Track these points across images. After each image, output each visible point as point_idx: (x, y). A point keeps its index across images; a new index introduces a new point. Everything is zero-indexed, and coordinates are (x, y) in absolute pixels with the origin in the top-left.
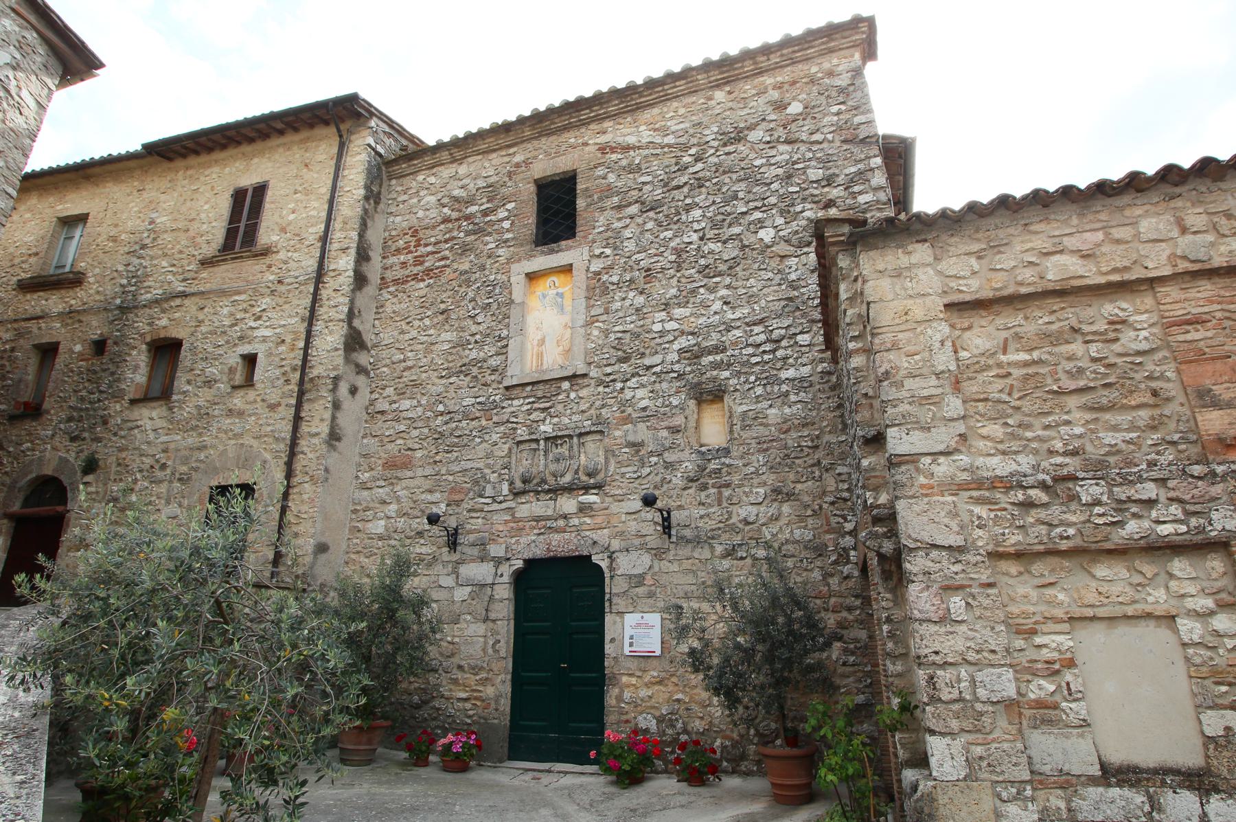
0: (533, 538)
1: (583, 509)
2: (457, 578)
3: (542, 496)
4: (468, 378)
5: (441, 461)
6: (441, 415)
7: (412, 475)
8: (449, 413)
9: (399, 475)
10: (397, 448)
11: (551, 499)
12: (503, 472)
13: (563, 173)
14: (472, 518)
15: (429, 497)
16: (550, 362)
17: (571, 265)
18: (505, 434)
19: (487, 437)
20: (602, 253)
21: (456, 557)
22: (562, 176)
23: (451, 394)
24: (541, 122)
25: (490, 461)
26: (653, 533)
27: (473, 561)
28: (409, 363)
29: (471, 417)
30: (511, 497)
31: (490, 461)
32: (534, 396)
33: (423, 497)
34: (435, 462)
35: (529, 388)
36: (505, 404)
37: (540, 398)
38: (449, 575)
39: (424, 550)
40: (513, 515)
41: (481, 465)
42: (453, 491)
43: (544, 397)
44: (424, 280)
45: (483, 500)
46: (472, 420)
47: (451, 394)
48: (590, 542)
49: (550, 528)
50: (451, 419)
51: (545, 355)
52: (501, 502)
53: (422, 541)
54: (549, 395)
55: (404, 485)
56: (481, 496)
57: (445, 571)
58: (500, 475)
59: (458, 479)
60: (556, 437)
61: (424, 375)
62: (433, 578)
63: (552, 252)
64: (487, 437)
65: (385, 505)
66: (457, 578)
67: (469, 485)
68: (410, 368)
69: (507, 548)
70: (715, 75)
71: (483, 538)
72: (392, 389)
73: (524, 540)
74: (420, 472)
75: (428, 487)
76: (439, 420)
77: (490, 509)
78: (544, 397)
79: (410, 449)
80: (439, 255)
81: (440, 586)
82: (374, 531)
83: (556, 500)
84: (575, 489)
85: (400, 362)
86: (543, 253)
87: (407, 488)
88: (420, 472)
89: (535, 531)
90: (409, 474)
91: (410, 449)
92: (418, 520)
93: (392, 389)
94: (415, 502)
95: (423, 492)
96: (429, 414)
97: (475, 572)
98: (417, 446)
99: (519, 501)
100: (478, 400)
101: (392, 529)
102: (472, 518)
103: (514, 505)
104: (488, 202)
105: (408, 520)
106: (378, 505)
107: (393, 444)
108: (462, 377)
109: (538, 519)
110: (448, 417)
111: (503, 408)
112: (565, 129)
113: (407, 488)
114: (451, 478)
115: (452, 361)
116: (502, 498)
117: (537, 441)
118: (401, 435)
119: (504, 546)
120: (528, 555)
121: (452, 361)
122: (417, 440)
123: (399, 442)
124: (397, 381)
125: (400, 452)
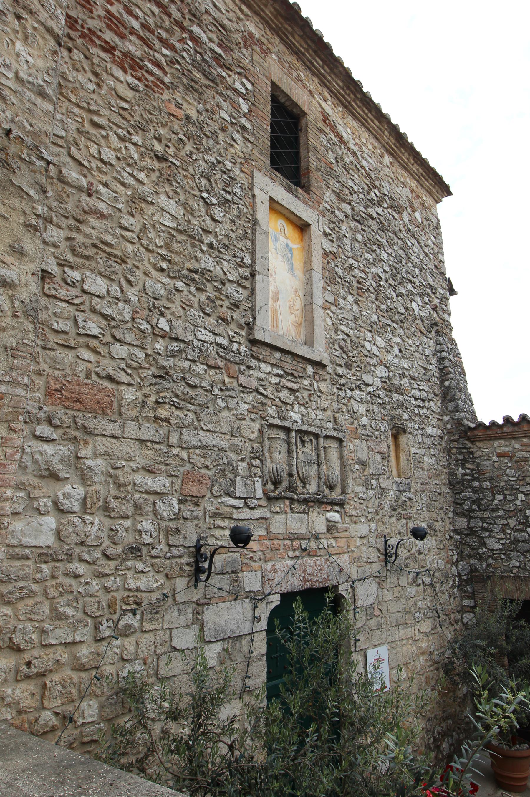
0: (290, 563)
1: (331, 527)
2: (202, 630)
3: (296, 505)
4: (202, 297)
5: (167, 421)
6: (163, 337)
7: (118, 432)
8: (177, 339)
9: (91, 424)
10: (83, 366)
11: (304, 512)
12: (254, 462)
13: (296, 105)
14: (217, 527)
15: (150, 483)
16: (285, 329)
17: (308, 225)
18: (254, 407)
19: (232, 404)
20: (330, 234)
21: (197, 595)
22: (287, 103)
23: (176, 307)
24: (286, 19)
25: (238, 442)
26: (377, 560)
27: (222, 599)
28: (102, 206)
29: (211, 362)
30: (264, 502)
31: (238, 442)
32: (283, 368)
33: (138, 478)
34: (157, 419)
35: (278, 355)
36: (253, 363)
37: (287, 374)
38: (187, 627)
39: (143, 583)
40: (268, 529)
41: (225, 444)
42: (187, 477)
43: (292, 375)
44: (125, 72)
45: (232, 502)
46: (210, 367)
47: (176, 307)
48: (337, 569)
49: (305, 550)
50: (180, 351)
51: (279, 312)
52: (253, 508)
53: (140, 566)
54: (296, 374)
55: (101, 448)
56: (229, 494)
57: (182, 621)
58: (250, 465)
59: (197, 460)
60: (306, 433)
61: (130, 248)
62: (162, 636)
63: (290, 191)
64: (232, 404)
65: (52, 483)
66: (202, 630)
67: (210, 473)
68: (101, 216)
69: (263, 577)
70: (392, 141)
71: (234, 561)
72: (62, 234)
73: (279, 565)
74: (131, 430)
75: (144, 462)
76: (160, 345)
77: (241, 516)
78: (292, 375)
79: (110, 378)
80: (151, 52)
81: (175, 649)
82: (26, 540)
83: (307, 513)
84: (323, 503)
85: (80, 189)
86: (281, 184)
87: (106, 455)
88: (131, 430)
89: (291, 554)
90: (111, 428)
91: (110, 378)
92: (127, 523)
93: (62, 234)
94: (119, 486)
95: (135, 471)
96: (145, 326)
97: (226, 617)
98: (124, 378)
99: (274, 509)
100: (219, 340)
101: (74, 538)
102: (217, 527)
103: (268, 515)
104: (220, 46)
105: (107, 522)
106: (36, 481)
107: (71, 356)
108: (193, 289)
109: (293, 537)
110: (175, 346)
111: (249, 367)
112: (296, 53)
113: (106, 455)
114: (184, 454)
115: (178, 253)
116: (255, 502)
117: (287, 430)
118: (93, 343)
119: (259, 574)
120: (286, 588)
121: (178, 253)
122: (123, 366)
123: (86, 354)
124: (73, 223)
125: (88, 376)
